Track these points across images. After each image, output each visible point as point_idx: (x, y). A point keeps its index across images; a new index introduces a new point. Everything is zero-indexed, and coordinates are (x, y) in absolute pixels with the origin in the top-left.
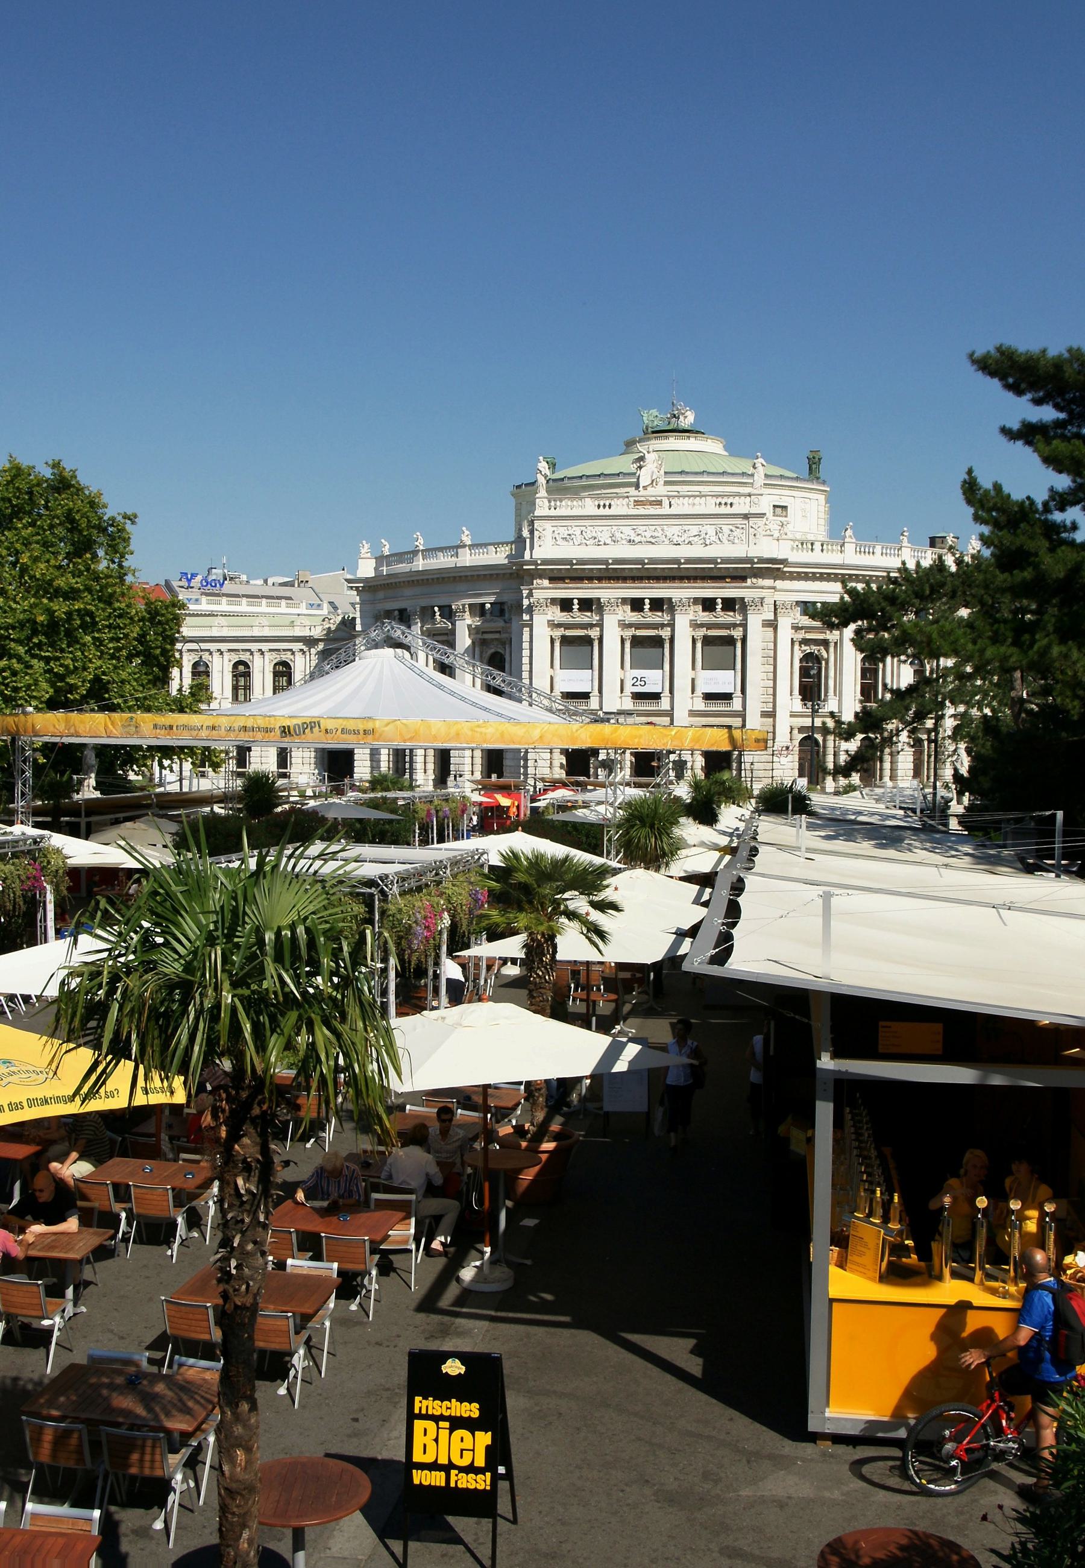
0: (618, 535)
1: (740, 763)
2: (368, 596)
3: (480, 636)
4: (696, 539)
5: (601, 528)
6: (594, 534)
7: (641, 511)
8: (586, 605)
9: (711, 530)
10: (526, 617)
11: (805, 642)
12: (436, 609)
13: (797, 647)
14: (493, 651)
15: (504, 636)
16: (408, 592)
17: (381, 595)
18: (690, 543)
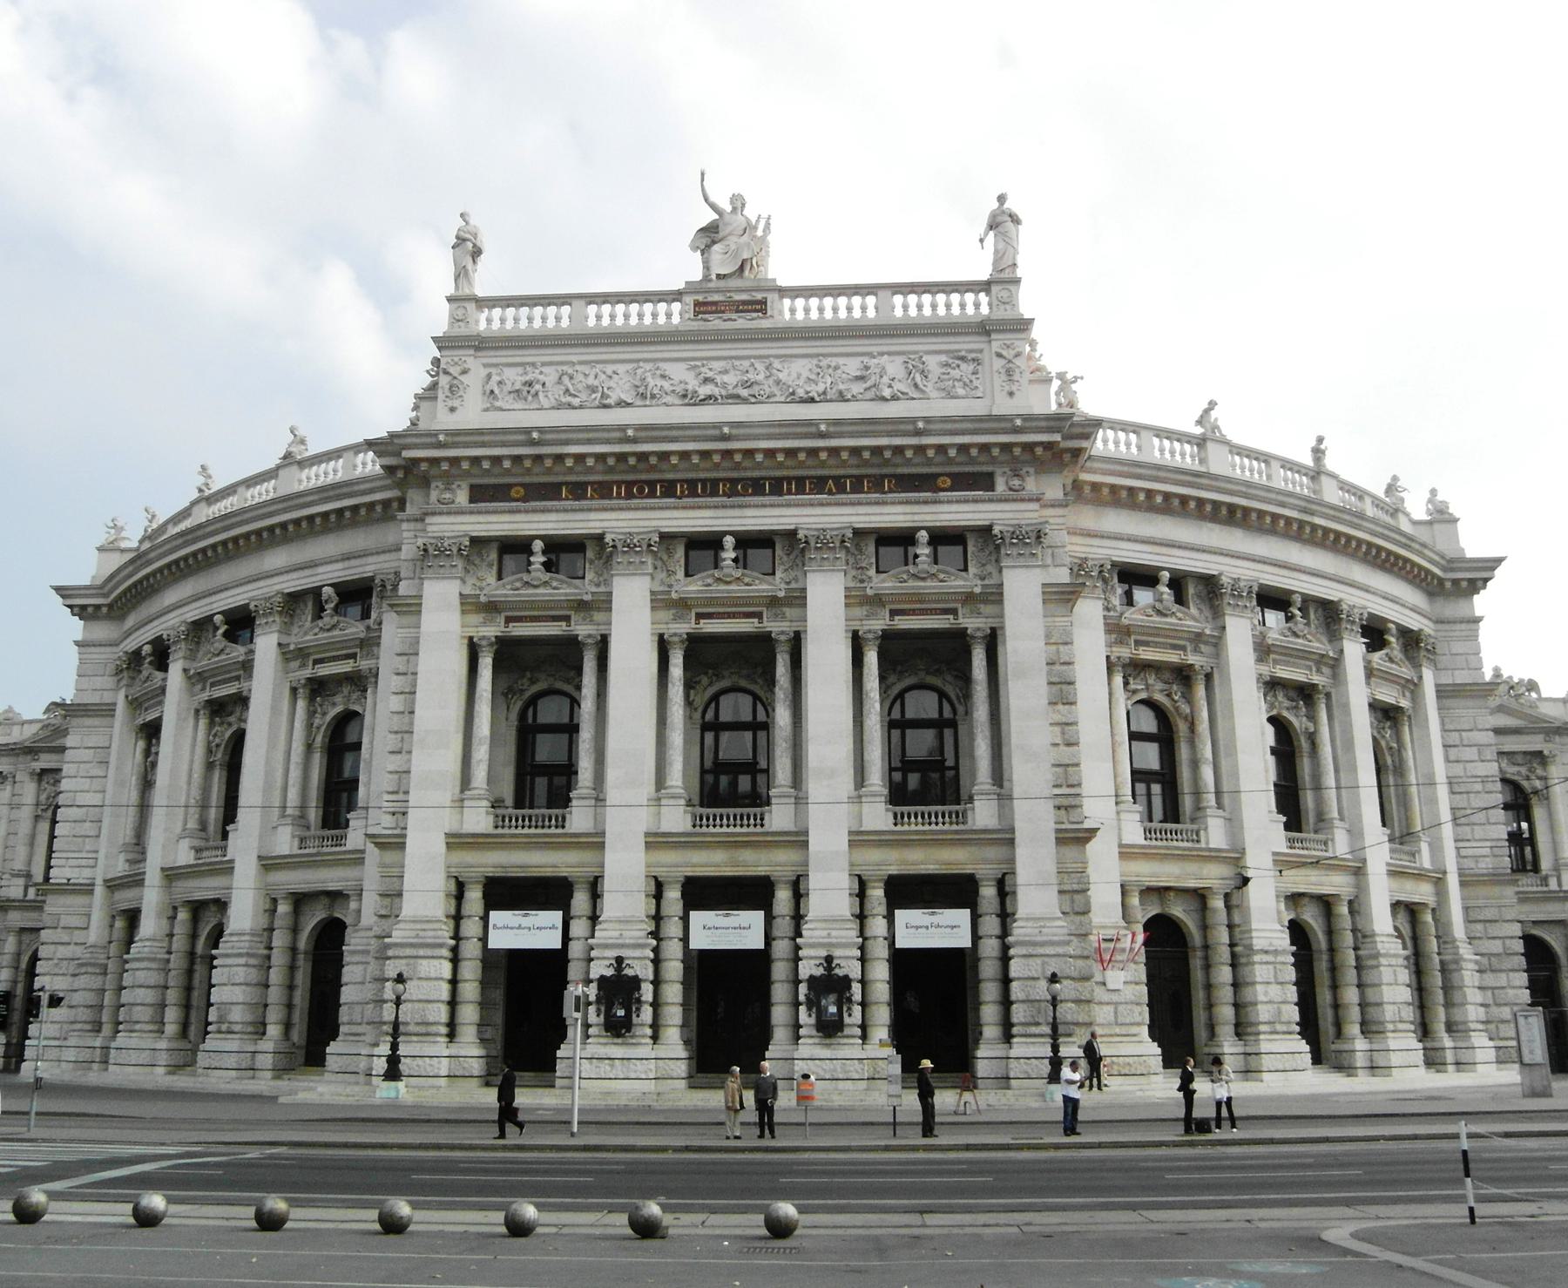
0: (651, 382)
1: (1006, 981)
2: (103, 631)
3: (308, 672)
4: (857, 388)
5: (609, 369)
6: (591, 381)
7: (716, 323)
8: (564, 552)
9: (894, 367)
10: (404, 588)
11: (1136, 668)
12: (218, 619)
13: (1118, 680)
14: (339, 709)
15: (364, 664)
16: (171, 596)
17: (131, 621)
18: (842, 398)
